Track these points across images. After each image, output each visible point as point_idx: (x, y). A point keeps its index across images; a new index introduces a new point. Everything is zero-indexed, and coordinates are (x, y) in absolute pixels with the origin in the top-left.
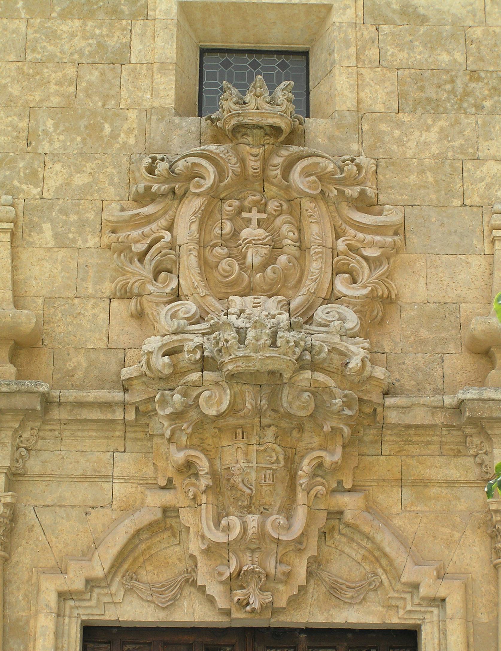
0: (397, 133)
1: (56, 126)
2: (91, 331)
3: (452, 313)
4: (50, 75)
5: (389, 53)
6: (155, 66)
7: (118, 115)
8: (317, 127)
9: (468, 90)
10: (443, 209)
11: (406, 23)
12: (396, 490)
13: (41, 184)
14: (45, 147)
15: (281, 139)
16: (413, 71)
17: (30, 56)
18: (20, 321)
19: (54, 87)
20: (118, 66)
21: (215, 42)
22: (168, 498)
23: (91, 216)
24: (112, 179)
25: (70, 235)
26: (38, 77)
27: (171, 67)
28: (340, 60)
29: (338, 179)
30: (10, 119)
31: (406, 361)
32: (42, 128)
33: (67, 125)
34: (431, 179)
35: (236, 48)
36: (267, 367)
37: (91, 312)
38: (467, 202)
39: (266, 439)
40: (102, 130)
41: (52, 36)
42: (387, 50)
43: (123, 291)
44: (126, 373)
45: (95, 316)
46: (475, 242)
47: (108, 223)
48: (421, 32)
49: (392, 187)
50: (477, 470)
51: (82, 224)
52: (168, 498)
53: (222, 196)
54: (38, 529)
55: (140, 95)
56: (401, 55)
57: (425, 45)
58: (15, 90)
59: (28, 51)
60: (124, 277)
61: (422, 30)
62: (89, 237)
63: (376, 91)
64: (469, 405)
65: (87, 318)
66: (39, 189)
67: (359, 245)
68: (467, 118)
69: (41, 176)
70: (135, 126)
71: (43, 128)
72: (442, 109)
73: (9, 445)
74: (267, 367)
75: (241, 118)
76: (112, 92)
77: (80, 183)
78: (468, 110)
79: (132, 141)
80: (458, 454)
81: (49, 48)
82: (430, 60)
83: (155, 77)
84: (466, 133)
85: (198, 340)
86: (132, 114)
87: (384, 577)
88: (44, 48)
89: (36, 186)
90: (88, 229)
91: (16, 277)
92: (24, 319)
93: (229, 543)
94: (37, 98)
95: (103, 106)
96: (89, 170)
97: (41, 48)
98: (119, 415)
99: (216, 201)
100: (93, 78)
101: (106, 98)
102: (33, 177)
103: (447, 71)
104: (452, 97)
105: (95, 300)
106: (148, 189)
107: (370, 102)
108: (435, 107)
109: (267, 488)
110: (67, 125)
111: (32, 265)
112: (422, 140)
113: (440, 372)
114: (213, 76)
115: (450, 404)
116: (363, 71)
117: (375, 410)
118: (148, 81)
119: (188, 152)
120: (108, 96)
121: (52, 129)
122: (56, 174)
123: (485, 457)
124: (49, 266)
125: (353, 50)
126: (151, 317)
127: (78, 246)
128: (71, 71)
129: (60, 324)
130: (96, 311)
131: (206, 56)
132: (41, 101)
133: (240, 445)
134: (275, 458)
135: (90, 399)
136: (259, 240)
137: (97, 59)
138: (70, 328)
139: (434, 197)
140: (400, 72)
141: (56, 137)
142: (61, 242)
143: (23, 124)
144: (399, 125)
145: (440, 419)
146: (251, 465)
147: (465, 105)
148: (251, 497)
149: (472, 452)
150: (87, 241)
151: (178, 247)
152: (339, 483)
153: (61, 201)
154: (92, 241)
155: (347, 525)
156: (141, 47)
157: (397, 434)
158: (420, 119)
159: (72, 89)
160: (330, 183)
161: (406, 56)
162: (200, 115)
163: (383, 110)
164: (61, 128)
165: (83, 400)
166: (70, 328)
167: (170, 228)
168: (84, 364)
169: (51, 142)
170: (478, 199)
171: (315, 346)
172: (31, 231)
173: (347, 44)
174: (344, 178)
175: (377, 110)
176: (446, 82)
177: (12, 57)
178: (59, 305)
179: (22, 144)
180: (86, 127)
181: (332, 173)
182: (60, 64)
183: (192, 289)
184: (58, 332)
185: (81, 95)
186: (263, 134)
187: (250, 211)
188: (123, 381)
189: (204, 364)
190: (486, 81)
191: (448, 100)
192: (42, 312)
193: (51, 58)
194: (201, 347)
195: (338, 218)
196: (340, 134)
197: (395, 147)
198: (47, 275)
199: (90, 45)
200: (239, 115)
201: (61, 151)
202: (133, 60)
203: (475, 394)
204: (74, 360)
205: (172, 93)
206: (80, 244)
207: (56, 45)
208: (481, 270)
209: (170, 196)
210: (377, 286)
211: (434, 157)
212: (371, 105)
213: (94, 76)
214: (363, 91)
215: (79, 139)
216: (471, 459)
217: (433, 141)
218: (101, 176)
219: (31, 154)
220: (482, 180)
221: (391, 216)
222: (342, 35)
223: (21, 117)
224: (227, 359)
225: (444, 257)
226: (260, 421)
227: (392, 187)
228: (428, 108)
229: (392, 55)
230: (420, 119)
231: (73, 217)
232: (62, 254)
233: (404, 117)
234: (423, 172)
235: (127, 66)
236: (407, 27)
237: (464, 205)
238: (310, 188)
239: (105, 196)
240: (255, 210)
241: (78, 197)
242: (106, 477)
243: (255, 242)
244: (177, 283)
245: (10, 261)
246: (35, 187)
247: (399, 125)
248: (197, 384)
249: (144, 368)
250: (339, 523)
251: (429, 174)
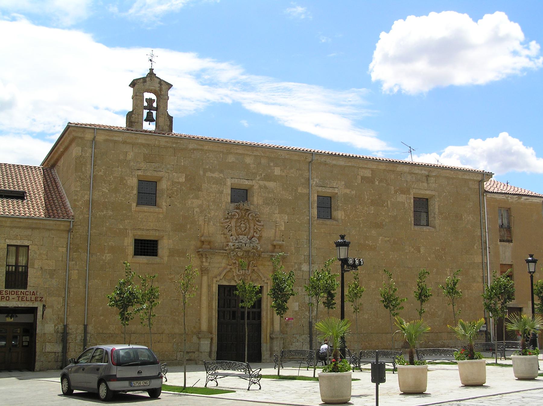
14: (211, 208)
41: (211, 188)
52: (231, 267)
102: (209, 213)
108: (268, 204)
112: (266, 210)
128: (214, 194)
142: (214, 224)
221: (262, 223)
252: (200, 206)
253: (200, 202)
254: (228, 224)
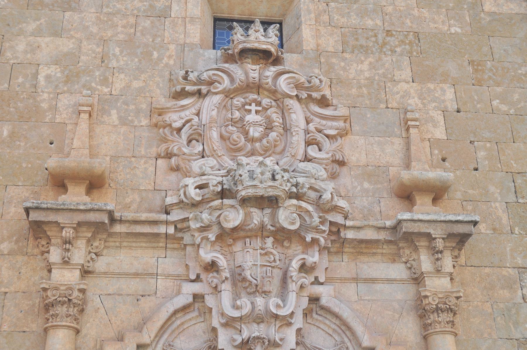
0: (343, 64)
1: (121, 52)
2: (143, 178)
3: (384, 172)
4: (118, 22)
5: (335, 19)
6: (187, 19)
7: (163, 47)
8: (290, 59)
9: (385, 41)
10: (374, 109)
11: (345, 2)
12: (354, 285)
13: (111, 86)
14: (114, 63)
15: (271, 60)
16: (351, 29)
17: (105, 10)
18: (94, 165)
19: (121, 28)
20: (163, 18)
21: (223, 14)
22: (197, 288)
23: (144, 106)
24: (158, 85)
25: (130, 118)
26: (110, 23)
27: (197, 20)
28: (305, 21)
29: (307, 87)
30: (90, 46)
31: (356, 202)
32: (112, 52)
33: (129, 51)
34: (365, 92)
35: (236, 19)
36: (269, 193)
37: (143, 166)
38: (389, 106)
39: (267, 246)
40: (152, 55)
42: (334, 17)
43: (165, 153)
44: (169, 200)
45: (146, 169)
46: (396, 130)
47: (156, 110)
48: (355, 8)
49: (341, 96)
50: (408, 272)
51: (138, 111)
52: (197, 288)
53: (231, 96)
54: (102, 311)
55: (177, 35)
56: (342, 20)
57: (357, 15)
58: (94, 29)
59: (104, 7)
60: (167, 144)
61: (355, 6)
62: (143, 119)
63: (328, 40)
64: (404, 224)
65: (141, 170)
66: (109, 89)
67: (323, 128)
68: (386, 57)
69: (111, 81)
70: (173, 53)
71: (113, 52)
72: (370, 52)
73: (84, 249)
74: (269, 193)
75: (245, 44)
76: (159, 33)
77: (137, 86)
78: (387, 53)
79: (172, 62)
80: (394, 261)
81: (118, 6)
82: (361, 23)
83: (187, 26)
84: (386, 66)
85: (220, 179)
86: (172, 47)
87: (349, 344)
88: (114, 6)
89: (107, 87)
90: (141, 115)
91: (91, 143)
92: (97, 165)
93: (242, 316)
94: (109, 35)
95: (153, 41)
96: (143, 79)
97: (112, 5)
98: (162, 229)
99: (228, 99)
100: (146, 25)
101: (155, 36)
103: (372, 30)
104: (376, 45)
105: (146, 159)
106: (183, 89)
107: (325, 46)
108: (366, 50)
109: (268, 279)
110: (129, 51)
111: (103, 135)
112: (359, 69)
113: (378, 209)
114: (222, 34)
115: (390, 226)
116: (320, 28)
117: (339, 230)
118: (182, 28)
119: (209, 68)
120: (156, 35)
121: (118, 53)
122: (121, 80)
123: (413, 262)
124: (114, 137)
125: (313, 15)
126: (184, 169)
127: (135, 125)
128: (132, 20)
129: (122, 173)
130: (146, 165)
131: (218, 22)
132: (112, 36)
133: (248, 250)
134: (273, 259)
135: (143, 219)
136: (257, 122)
137: (149, 14)
138: (128, 176)
139: (368, 102)
140: (342, 30)
141: (121, 58)
142: (123, 121)
143: (99, 50)
144: (344, 59)
145: (382, 236)
146: (256, 263)
147: (385, 50)
148: (257, 286)
149: (404, 260)
150: (141, 122)
151: (203, 126)
152: (316, 278)
153: (123, 97)
154: (145, 122)
155: (322, 308)
156: (178, 8)
157: (353, 248)
158: (356, 57)
159: (132, 30)
160: (302, 90)
161: (346, 21)
163: (333, 51)
164: (125, 53)
165: (138, 219)
166: (128, 176)
167: (198, 114)
168: (138, 200)
169: (118, 61)
170: (396, 105)
171: (299, 183)
172: (103, 114)
173: (309, 12)
174: (312, 87)
175: (329, 50)
176: (372, 36)
177: (93, 10)
178: (121, 162)
179: (98, 61)
180: (142, 53)
181: (303, 83)
182: (125, 16)
183: (212, 152)
184: (119, 178)
185: (138, 34)
186: (258, 58)
187: (250, 105)
188: (166, 206)
189: (223, 194)
190: (396, 36)
191: (374, 46)
192: (109, 166)
193: (118, 12)
194: (221, 183)
195: (308, 112)
196: (307, 63)
197: (342, 72)
198: (113, 142)
199: (145, 6)
200: (244, 42)
201: (125, 67)
202: (173, 15)
203: (409, 216)
204: (131, 197)
205: (198, 35)
206: (136, 123)
207: (122, 4)
208: (401, 147)
209: (197, 95)
210: (335, 153)
211: (367, 79)
212: (325, 47)
213: (147, 23)
214: (320, 39)
215: (136, 60)
216: (403, 265)
217: (366, 69)
218: (151, 83)
219: (104, 68)
220: (398, 93)
221: (342, 111)
222: (306, 7)
223: (98, 45)
224: (240, 188)
225: (377, 139)
226: (262, 234)
227: (341, 96)
228: (362, 50)
229: (337, 20)
230: (356, 57)
231: (132, 107)
232: (123, 129)
233: (347, 55)
234: (360, 87)
235: (168, 19)
236: (345, 4)
237: (387, 108)
238: (289, 91)
239: (154, 95)
240: (253, 104)
241: (135, 94)
242: (152, 274)
243: (255, 124)
244: (202, 148)
245: (88, 131)
246: (106, 88)
247: (344, 59)
248: (218, 207)
249: (182, 196)
250: (316, 307)
251: (364, 89)
252: (67, 62)
253: (66, 45)
254: (187, 114)
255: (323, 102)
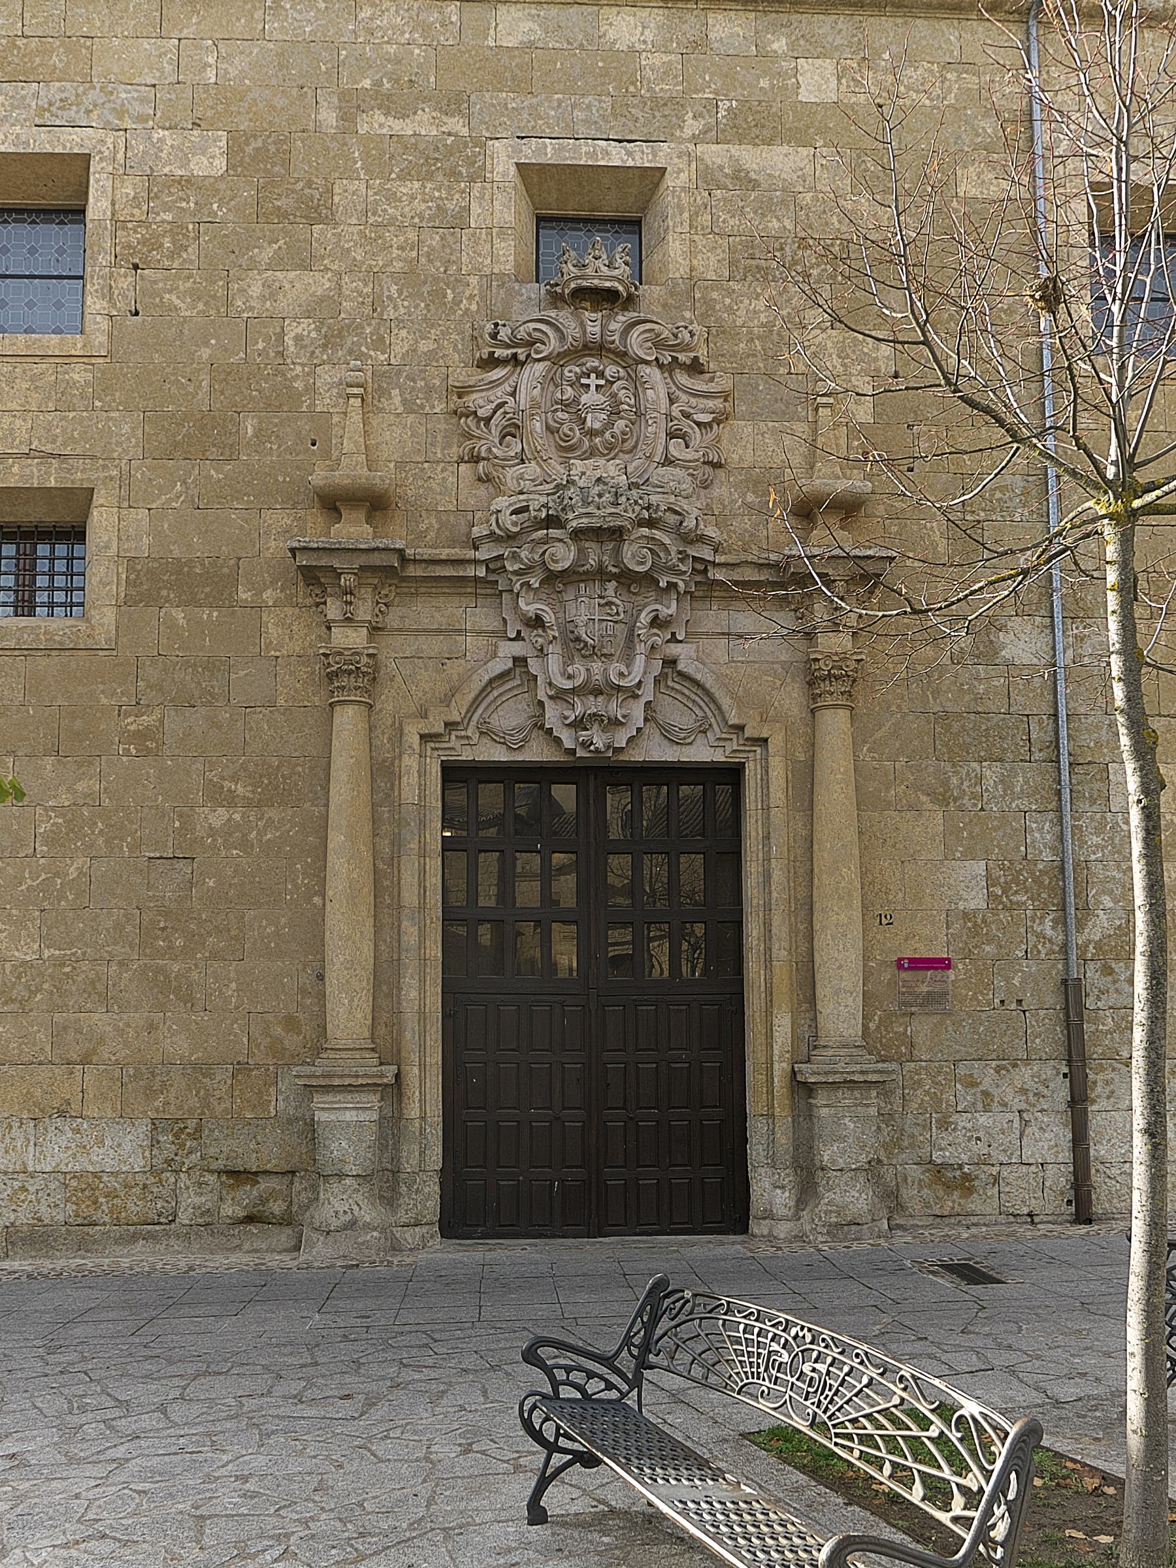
0: (728, 301)
8: (651, 294)
14: (390, 313)
22: (518, 649)
40: (445, 296)
41: (392, 198)
44: (476, 531)
49: (722, 356)
51: (429, 390)
52: (518, 649)
54: (399, 679)
58: (358, 255)
67: (692, 411)
70: (476, 292)
73: (369, 601)
76: (453, 258)
79: (474, 307)
85: (543, 499)
86: (474, 280)
88: (385, 210)
89: (383, 353)
92: (378, 481)
93: (574, 688)
95: (445, 271)
98: (470, 572)
102: (380, 343)
108: (765, 275)
112: (751, 309)
116: (696, 238)
121: (396, 295)
125: (686, 215)
128: (412, 235)
135: (443, 557)
139: (761, 365)
142: (410, 407)
152: (673, 634)
155: (680, 674)
159: (414, 254)
162: (537, 281)
164: (405, 293)
165: (437, 558)
166: (421, 491)
167: (513, 394)
169: (396, 308)
179: (368, 310)
185: (423, 260)
193: (392, 221)
194: (545, 506)
199: (430, 208)
207: (396, 207)
211: (763, 325)
215: (423, 305)
221: (724, 382)
224: (571, 516)
225: (770, 424)
227: (722, 356)
228: (758, 276)
242: (460, 630)
243: (593, 408)
253: (321, 283)
254: (499, 394)
255: (695, 368)
